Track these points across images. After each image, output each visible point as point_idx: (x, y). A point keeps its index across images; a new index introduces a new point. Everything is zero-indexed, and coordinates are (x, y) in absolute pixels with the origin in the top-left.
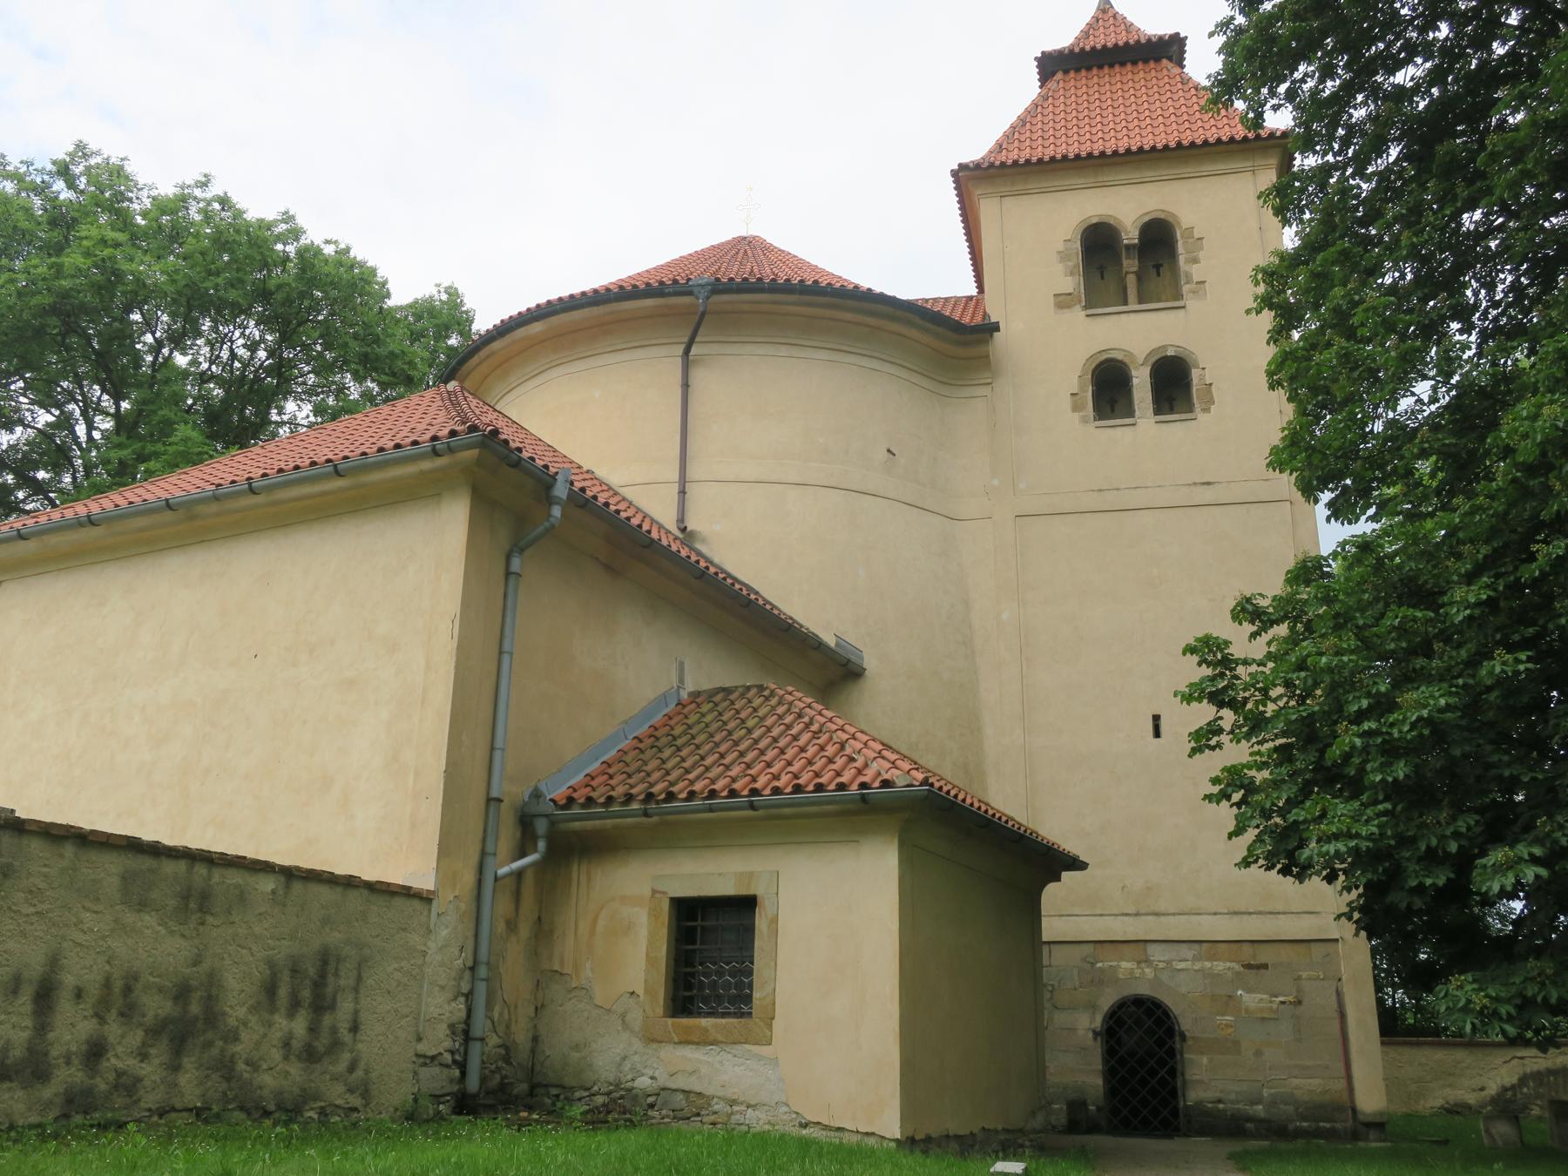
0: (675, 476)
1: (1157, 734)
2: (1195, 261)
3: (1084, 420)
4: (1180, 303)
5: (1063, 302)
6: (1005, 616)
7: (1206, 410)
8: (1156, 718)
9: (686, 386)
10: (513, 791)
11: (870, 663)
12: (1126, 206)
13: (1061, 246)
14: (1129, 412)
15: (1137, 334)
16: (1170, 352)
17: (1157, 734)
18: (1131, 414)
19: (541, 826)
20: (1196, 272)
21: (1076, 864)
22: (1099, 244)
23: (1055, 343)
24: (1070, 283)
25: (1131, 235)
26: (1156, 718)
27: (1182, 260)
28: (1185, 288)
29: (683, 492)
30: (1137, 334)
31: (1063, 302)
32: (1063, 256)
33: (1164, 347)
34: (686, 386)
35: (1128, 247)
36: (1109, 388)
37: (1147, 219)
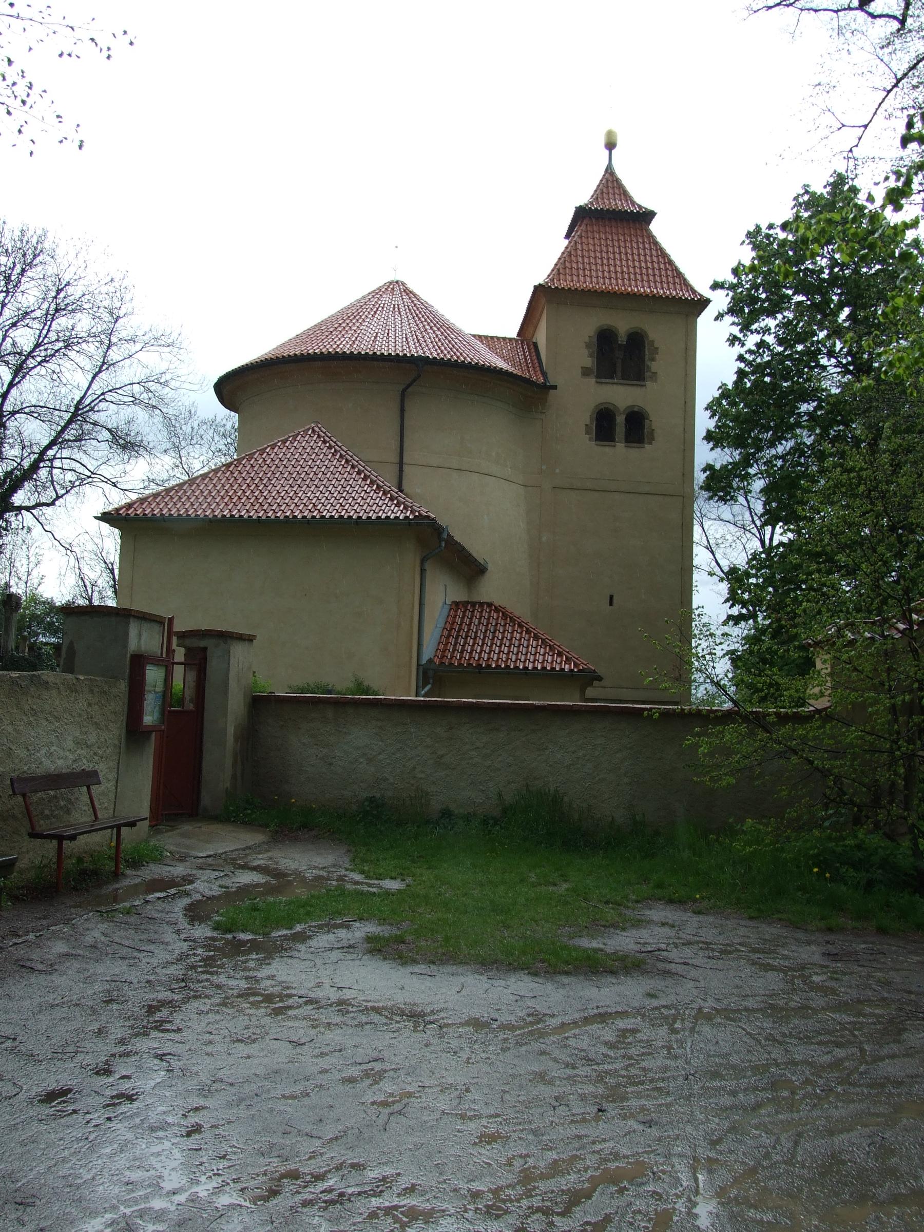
0: (397, 460)
1: (611, 604)
2: (653, 360)
3: (590, 439)
4: (642, 383)
5: (586, 372)
6: (544, 539)
7: (651, 443)
8: (611, 597)
9: (402, 410)
10: (424, 661)
11: (490, 567)
12: (623, 324)
13: (587, 340)
14: (612, 439)
15: (622, 396)
16: (636, 409)
17: (611, 604)
18: (613, 440)
19: (431, 673)
20: (654, 366)
21: (599, 678)
22: (605, 338)
23: (579, 394)
24: (589, 362)
25: (622, 339)
26: (611, 597)
27: (647, 357)
28: (648, 374)
29: (401, 471)
30: (622, 396)
31: (586, 372)
32: (588, 346)
33: (634, 406)
34: (402, 410)
35: (620, 345)
36: (604, 425)
37: (632, 331)
